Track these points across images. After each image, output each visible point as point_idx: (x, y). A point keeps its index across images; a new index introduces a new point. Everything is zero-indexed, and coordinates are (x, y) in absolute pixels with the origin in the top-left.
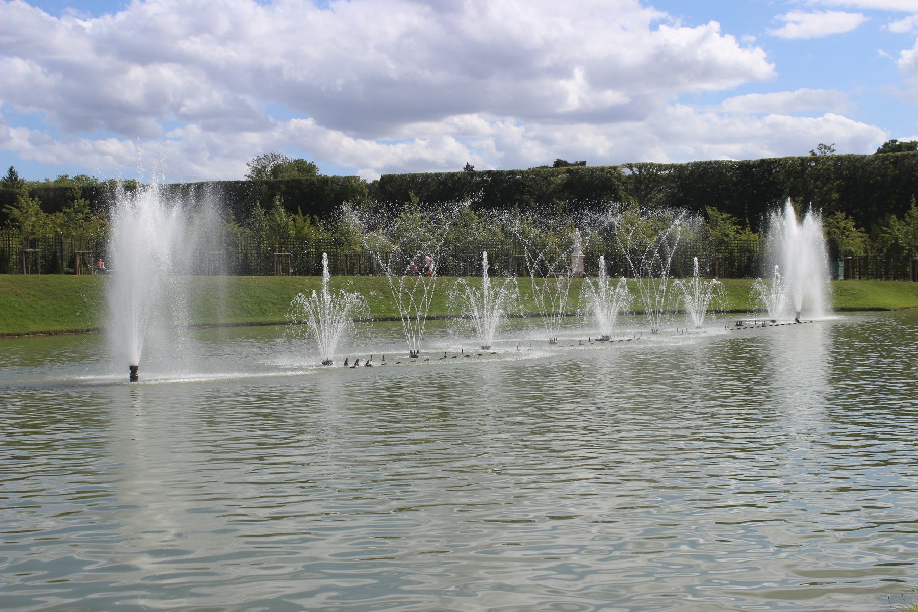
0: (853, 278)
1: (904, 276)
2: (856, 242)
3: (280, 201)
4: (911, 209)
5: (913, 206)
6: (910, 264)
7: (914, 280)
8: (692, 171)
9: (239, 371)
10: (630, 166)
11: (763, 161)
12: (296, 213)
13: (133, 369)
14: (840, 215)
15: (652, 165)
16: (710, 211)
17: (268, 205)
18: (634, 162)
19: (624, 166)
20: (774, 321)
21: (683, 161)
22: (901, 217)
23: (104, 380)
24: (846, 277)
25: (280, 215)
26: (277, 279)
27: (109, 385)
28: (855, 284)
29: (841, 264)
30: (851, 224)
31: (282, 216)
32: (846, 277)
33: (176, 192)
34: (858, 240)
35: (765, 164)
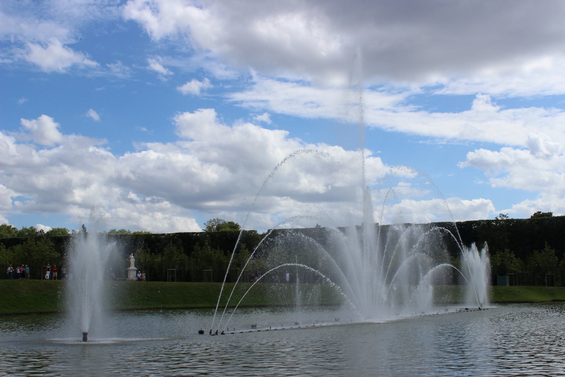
0: (516, 285)
1: (544, 284)
2: (515, 264)
3: (208, 242)
4: (545, 247)
6: (546, 277)
7: (548, 286)
9: (136, 336)
11: (467, 222)
12: (216, 249)
14: (507, 250)
17: (202, 245)
19: (394, 225)
20: (254, 326)
22: (540, 252)
23: (57, 341)
24: (511, 284)
25: (207, 249)
26: (204, 284)
28: (516, 288)
29: (508, 277)
30: (513, 255)
31: (209, 250)
32: (511, 284)
34: (518, 264)
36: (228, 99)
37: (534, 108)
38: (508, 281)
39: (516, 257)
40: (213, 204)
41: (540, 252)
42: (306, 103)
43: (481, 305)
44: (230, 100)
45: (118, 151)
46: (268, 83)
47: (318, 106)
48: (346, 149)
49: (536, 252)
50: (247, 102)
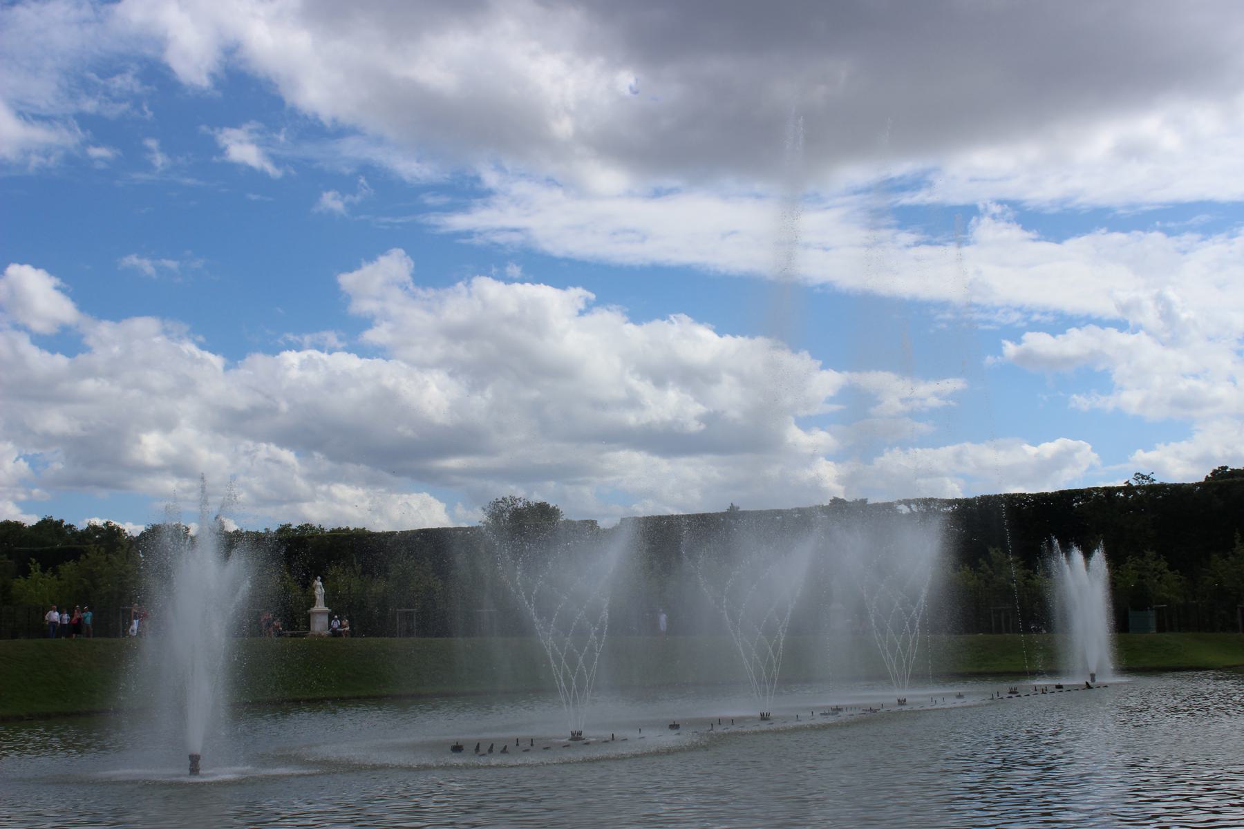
1: (1234, 628)
4: (1234, 545)
5: (1237, 542)
8: (981, 506)
10: (907, 502)
11: (1062, 492)
13: (194, 759)
14: (1149, 553)
15: (931, 499)
16: (992, 551)
18: (911, 498)
19: (900, 502)
21: (971, 496)
22: (1226, 557)
24: (1161, 629)
27: (127, 782)
28: (1170, 638)
29: (1152, 614)
30: (1163, 565)
32: (1161, 629)
33: (231, 542)
35: (1065, 497)
36: (437, 227)
37: (1140, 233)
38: (1153, 623)
39: (1171, 569)
40: (454, 463)
41: (1226, 557)
42: (614, 234)
43: (1093, 676)
44: (443, 231)
45: (234, 354)
46: (521, 188)
47: (644, 238)
48: (720, 332)
49: (1215, 556)
50: (480, 234)
